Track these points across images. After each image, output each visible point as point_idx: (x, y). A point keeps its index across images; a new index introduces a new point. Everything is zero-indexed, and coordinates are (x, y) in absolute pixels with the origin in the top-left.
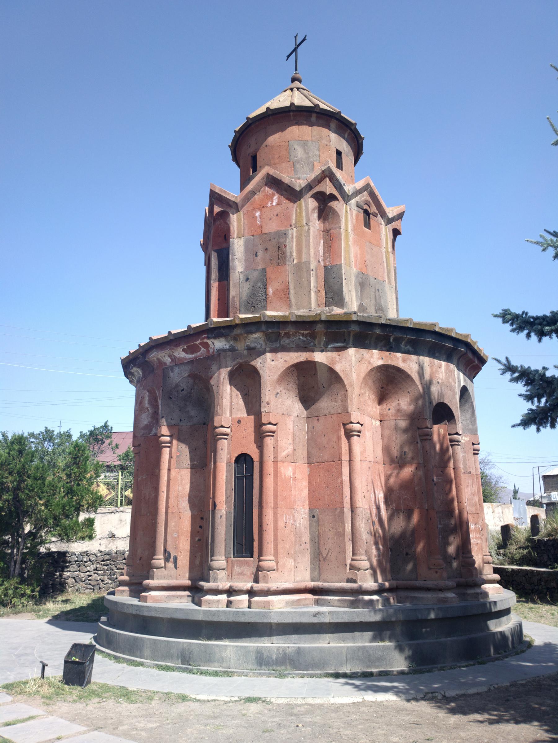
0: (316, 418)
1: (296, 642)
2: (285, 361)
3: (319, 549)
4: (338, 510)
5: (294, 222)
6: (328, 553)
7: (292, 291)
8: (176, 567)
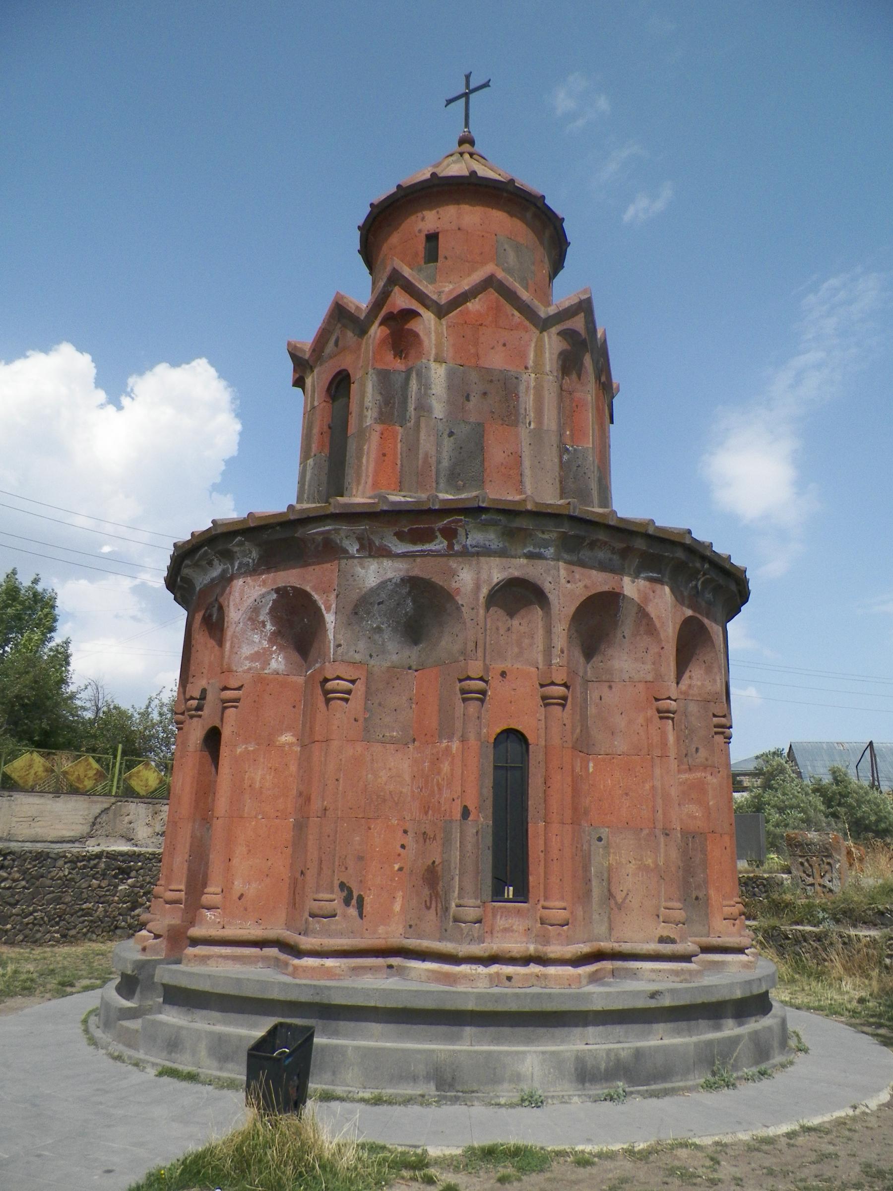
0: (607, 684)
1: (621, 1040)
2: (586, 587)
3: (609, 890)
4: (646, 832)
5: (531, 363)
6: (625, 899)
7: (527, 472)
8: (361, 915)
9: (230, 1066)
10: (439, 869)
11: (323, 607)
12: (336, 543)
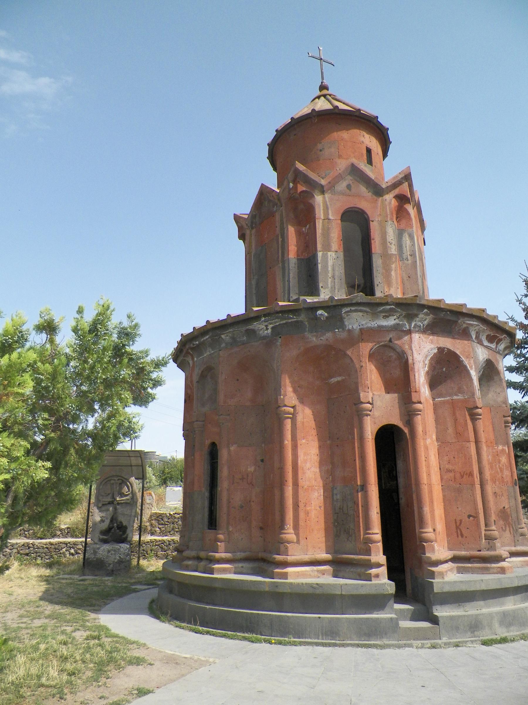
9: (512, 628)
10: (508, 510)
11: (468, 366)
12: (469, 331)
